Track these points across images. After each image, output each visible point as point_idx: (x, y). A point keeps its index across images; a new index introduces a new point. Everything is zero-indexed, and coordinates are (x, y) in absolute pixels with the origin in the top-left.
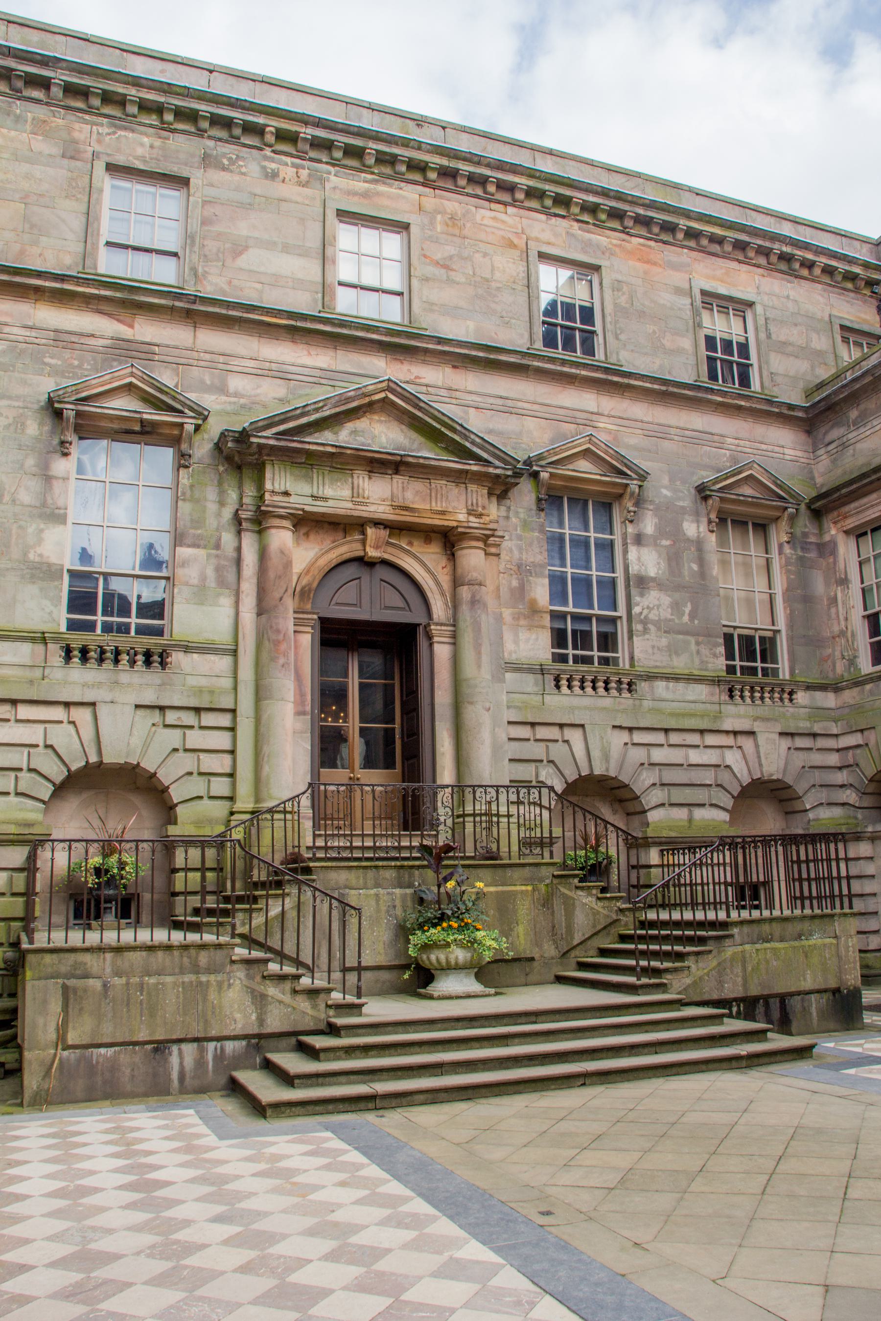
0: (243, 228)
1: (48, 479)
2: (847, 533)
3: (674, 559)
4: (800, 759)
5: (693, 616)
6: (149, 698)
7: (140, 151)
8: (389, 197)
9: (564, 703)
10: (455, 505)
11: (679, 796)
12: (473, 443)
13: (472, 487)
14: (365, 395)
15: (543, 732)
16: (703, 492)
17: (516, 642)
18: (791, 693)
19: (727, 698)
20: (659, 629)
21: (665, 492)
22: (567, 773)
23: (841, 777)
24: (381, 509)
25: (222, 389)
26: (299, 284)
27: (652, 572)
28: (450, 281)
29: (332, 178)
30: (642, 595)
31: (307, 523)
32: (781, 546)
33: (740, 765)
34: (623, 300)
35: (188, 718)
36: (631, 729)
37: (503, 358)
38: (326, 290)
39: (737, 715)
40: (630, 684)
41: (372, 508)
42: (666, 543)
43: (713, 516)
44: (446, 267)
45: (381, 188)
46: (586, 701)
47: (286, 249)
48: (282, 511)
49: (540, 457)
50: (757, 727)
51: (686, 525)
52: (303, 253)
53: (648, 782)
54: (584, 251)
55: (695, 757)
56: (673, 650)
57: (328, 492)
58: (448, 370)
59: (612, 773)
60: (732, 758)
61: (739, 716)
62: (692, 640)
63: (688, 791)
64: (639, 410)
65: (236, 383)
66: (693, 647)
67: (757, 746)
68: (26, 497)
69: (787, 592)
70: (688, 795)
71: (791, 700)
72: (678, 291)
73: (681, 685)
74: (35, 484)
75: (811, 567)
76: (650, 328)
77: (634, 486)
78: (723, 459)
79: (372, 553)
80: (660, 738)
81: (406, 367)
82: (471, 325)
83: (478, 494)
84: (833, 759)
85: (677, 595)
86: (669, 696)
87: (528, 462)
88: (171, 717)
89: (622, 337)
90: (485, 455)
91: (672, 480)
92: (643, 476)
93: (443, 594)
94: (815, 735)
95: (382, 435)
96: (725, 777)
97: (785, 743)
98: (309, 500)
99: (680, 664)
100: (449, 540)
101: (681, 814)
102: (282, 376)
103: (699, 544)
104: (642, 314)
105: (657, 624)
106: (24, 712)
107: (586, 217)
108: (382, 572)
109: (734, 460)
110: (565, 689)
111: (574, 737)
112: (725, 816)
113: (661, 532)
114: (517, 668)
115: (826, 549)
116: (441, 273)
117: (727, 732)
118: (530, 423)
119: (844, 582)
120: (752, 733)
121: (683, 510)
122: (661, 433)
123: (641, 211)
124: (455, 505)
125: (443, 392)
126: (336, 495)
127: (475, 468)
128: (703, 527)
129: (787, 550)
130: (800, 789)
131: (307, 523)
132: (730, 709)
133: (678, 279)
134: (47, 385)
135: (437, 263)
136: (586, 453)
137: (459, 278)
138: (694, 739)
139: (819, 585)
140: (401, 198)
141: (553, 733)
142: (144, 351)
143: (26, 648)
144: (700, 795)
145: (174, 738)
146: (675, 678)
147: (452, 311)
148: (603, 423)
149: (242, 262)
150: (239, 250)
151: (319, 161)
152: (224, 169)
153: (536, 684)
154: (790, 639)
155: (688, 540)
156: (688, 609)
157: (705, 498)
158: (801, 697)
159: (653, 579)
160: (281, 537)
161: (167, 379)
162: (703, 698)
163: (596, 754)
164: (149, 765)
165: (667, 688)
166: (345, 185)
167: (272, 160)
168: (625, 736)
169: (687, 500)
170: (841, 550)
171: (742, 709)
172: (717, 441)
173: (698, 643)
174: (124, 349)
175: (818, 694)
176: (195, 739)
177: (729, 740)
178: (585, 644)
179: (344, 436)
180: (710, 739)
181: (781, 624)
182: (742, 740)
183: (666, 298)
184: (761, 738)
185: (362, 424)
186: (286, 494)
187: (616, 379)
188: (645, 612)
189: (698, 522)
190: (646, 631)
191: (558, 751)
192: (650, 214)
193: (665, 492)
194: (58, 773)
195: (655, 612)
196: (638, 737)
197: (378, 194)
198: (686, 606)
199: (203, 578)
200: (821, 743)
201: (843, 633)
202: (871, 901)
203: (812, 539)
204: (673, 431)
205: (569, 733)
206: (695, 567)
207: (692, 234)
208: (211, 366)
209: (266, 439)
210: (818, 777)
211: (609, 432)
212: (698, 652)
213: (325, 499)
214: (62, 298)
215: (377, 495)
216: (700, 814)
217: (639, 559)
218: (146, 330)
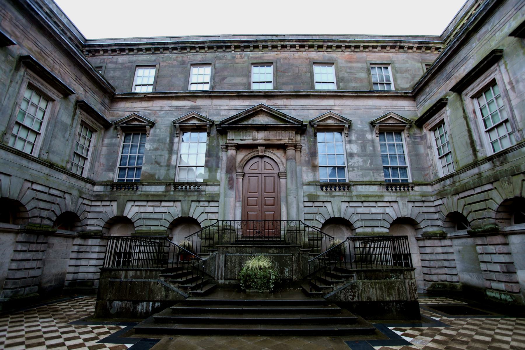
2: (430, 130)
3: (363, 147)
4: (417, 210)
5: (371, 164)
8: (267, 56)
10: (284, 138)
11: (368, 223)
12: (288, 118)
13: (290, 131)
14: (254, 110)
15: (317, 204)
16: (373, 124)
17: (307, 176)
18: (412, 187)
19: (386, 190)
20: (358, 169)
21: (359, 126)
22: (326, 217)
23: (436, 216)
24: (261, 141)
27: (355, 151)
30: (352, 159)
31: (239, 147)
32: (405, 139)
33: (393, 213)
35: (206, 204)
36: (349, 202)
38: (249, 85)
39: (389, 196)
41: (258, 141)
42: (359, 142)
43: (377, 132)
45: (265, 55)
48: (231, 145)
50: (398, 199)
51: (367, 136)
55: (373, 210)
57: (245, 138)
58: (285, 100)
59: (342, 217)
60: (388, 210)
62: (371, 172)
63: (371, 222)
66: (372, 174)
67: (399, 206)
69: (409, 153)
71: (412, 190)
73: (367, 187)
75: (418, 144)
77: (347, 126)
78: (381, 113)
79: (260, 154)
80: (360, 204)
81: (272, 101)
83: (292, 133)
84: (433, 210)
85: (365, 158)
86: (363, 190)
87: (310, 122)
88: (202, 204)
90: (292, 121)
91: (361, 122)
92: (349, 122)
93: (283, 164)
94: (423, 201)
95: (262, 120)
96: (386, 217)
97: (410, 205)
98: (240, 141)
100: (283, 147)
105: (358, 168)
106: (163, 204)
107: (329, 50)
108: (266, 159)
111: (328, 205)
112: (387, 231)
113: (358, 139)
115: (423, 138)
117: (386, 202)
119: (430, 147)
120: (396, 202)
121: (366, 131)
122: (358, 108)
123: (347, 44)
124: (284, 138)
126: (248, 138)
127: (289, 125)
128: (374, 135)
129: (408, 139)
130: (418, 220)
131: (239, 147)
132: (388, 194)
135: (281, 71)
136: (330, 117)
138: (373, 204)
139: (422, 149)
142: (199, 108)
144: (379, 223)
145: (201, 209)
147: (285, 84)
148: (336, 108)
149: (225, 81)
150: (224, 79)
151: (247, 52)
153: (314, 189)
154: (411, 169)
155: (368, 140)
156: (369, 162)
157: (374, 126)
160: (232, 152)
161: (204, 114)
162: (376, 190)
163: (336, 210)
164: (195, 217)
165: (362, 188)
169: (367, 128)
170: (428, 136)
172: (379, 108)
173: (373, 173)
174: (193, 108)
175: (424, 187)
176: (208, 210)
177: (388, 204)
179: (250, 122)
180: (380, 204)
181: (408, 164)
182: (392, 204)
184: (400, 203)
185: (255, 118)
186: (233, 140)
187: (339, 94)
188: (353, 164)
189: (372, 134)
190: (353, 170)
191: (322, 210)
192: (350, 44)
193: (359, 126)
194: (171, 220)
195: (357, 164)
196: (351, 204)
197: (264, 56)
198: (368, 161)
200: (426, 204)
201: (432, 165)
202: (452, 262)
203: (418, 135)
204: (361, 107)
206: (371, 148)
207: (365, 47)
208: (216, 109)
209: (226, 125)
210: (426, 216)
211: (339, 110)
212: (373, 176)
213: (245, 140)
214: (178, 98)
215: (260, 137)
217: (350, 148)
218: (200, 102)
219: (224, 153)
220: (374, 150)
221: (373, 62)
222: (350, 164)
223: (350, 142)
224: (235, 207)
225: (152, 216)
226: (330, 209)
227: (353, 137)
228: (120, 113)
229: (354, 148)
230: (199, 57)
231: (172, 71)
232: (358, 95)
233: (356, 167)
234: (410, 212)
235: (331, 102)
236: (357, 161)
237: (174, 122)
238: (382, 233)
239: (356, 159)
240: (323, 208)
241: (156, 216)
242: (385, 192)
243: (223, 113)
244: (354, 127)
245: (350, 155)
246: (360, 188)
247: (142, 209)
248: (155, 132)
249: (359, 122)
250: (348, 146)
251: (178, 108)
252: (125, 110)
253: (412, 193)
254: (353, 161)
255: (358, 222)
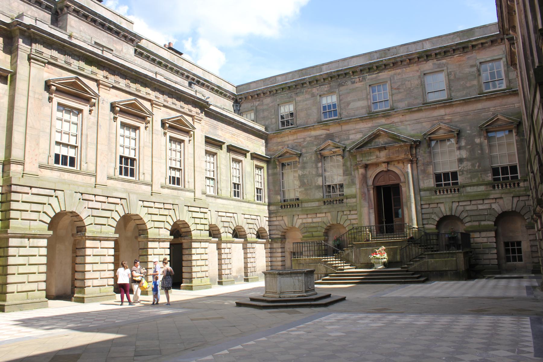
0: (349, 99)
1: (317, 168)
3: (472, 151)
4: (521, 204)
5: (479, 167)
6: (340, 209)
7: (326, 89)
9: (440, 197)
15: (432, 206)
17: (424, 183)
21: (468, 132)
25: (348, 139)
26: (363, 108)
28: (400, 93)
29: (368, 77)
30: (461, 164)
33: (497, 208)
34: (452, 77)
36: (459, 202)
37: (413, 110)
39: (496, 193)
40: (458, 190)
42: (468, 147)
44: (398, 89)
45: (380, 74)
46: (444, 196)
47: (359, 100)
49: (425, 135)
50: (503, 196)
51: (476, 140)
52: (363, 99)
53: (465, 216)
54: (439, 67)
55: (480, 207)
56: (471, 178)
59: (453, 214)
60: (494, 206)
61: (496, 193)
63: (478, 217)
64: (459, 109)
65: (351, 137)
66: (480, 176)
68: (314, 173)
70: (479, 218)
72: (472, 66)
73: (475, 187)
74: (315, 170)
76: (462, 83)
78: (489, 115)
82: (406, 102)
86: (472, 191)
89: (452, 89)
97: (515, 200)
99: (475, 181)
101: (477, 223)
102: (361, 132)
103: (481, 144)
104: (458, 79)
105: (466, 171)
109: (493, 114)
110: (438, 193)
113: (467, 144)
114: (425, 190)
116: (397, 91)
118: (424, 124)
120: (501, 198)
125: (400, 123)
131: (366, 167)
132: (493, 192)
133: (471, 62)
134: (315, 148)
135: (396, 89)
137: (402, 90)
140: (384, 75)
141: (435, 205)
143: (317, 203)
145: (345, 217)
146: (474, 185)
147: (400, 101)
149: (350, 107)
150: (348, 104)
152: (343, 86)
155: (477, 144)
158: (521, 184)
159: (465, 158)
162: (483, 189)
166: (370, 77)
167: (353, 79)
168: (457, 204)
171: (498, 191)
173: (481, 174)
176: (350, 217)
177: (494, 201)
178: (446, 181)
180: (486, 201)
183: (467, 70)
184: (505, 199)
186: (362, 161)
190: (463, 174)
191: (436, 210)
193: (468, 132)
196: (461, 204)
199: (349, 182)
205: (439, 205)
206: (479, 152)
211: (449, 119)
216: (483, 223)
219: (356, 172)
220: (482, 153)
221: (483, 60)
222: (460, 168)
223: (459, 148)
224: (369, 213)
225: (312, 225)
226: (443, 209)
227: (463, 143)
228: (275, 148)
229: (464, 154)
230: (326, 88)
231: (306, 104)
232: (466, 102)
233: (466, 171)
234: (514, 206)
235: (442, 112)
236: (467, 165)
237: (316, 151)
238: (488, 225)
239: (465, 163)
240: (438, 209)
241: (314, 225)
242: (491, 190)
243: (351, 137)
244: (463, 134)
245: (461, 160)
246: (469, 189)
247: (304, 221)
248: (303, 160)
249: (468, 128)
250: (457, 153)
251: (316, 137)
252: (278, 144)
253: (517, 189)
254: (462, 166)
255: (467, 218)
